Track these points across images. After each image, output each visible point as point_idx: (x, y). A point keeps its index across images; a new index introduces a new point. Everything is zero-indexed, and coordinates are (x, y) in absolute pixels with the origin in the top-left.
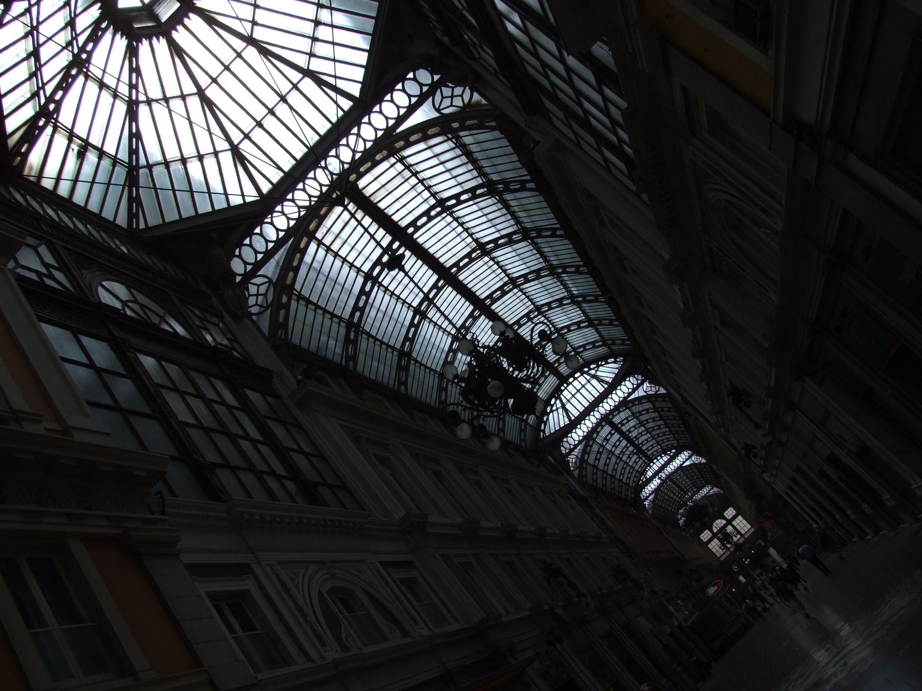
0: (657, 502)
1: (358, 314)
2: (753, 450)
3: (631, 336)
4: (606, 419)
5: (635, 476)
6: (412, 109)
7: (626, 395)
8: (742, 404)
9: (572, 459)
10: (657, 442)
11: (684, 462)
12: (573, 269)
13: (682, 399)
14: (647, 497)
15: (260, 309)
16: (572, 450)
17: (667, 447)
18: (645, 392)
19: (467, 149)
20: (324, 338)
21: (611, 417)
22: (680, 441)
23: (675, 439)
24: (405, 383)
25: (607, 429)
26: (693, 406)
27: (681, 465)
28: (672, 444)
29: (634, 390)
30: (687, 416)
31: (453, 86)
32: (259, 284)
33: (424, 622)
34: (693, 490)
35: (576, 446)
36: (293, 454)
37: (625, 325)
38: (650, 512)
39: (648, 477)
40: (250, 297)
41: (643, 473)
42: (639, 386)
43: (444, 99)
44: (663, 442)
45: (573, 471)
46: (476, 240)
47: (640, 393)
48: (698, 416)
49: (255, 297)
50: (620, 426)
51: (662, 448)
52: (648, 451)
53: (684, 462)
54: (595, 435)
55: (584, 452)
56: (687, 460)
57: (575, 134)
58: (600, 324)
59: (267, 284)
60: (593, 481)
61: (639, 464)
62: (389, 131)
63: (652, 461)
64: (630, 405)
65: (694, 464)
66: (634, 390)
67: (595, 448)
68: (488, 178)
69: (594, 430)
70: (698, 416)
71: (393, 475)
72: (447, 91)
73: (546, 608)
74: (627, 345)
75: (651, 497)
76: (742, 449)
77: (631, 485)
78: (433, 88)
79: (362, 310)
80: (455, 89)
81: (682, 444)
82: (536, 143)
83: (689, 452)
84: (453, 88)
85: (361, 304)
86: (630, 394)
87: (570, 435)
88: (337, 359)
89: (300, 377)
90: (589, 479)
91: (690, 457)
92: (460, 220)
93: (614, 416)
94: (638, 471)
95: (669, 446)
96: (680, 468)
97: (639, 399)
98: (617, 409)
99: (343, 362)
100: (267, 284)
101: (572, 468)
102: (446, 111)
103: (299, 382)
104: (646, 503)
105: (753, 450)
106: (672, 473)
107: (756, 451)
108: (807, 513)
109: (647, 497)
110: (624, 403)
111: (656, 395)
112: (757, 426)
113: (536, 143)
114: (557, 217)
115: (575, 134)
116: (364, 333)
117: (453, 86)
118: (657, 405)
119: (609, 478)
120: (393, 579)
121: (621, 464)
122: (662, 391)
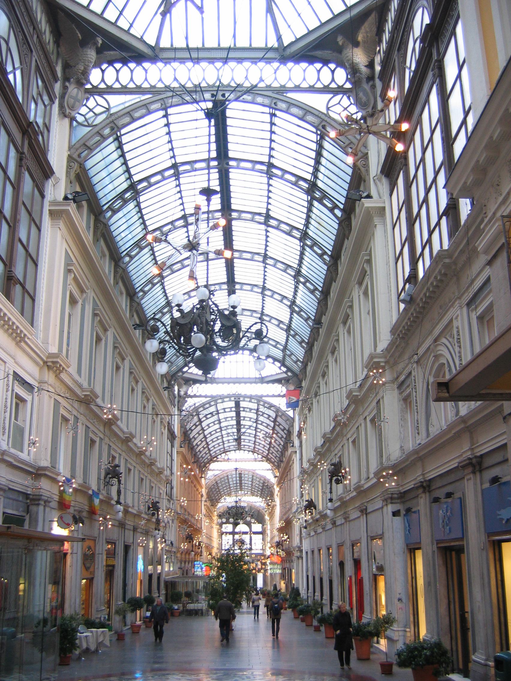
1: (145, 184)
2: (312, 508)
3: (305, 364)
5: (220, 449)
6: (312, 89)
8: (335, 478)
9: (190, 403)
10: (255, 441)
12: (312, 287)
13: (298, 432)
15: (84, 121)
16: (195, 396)
17: (258, 451)
19: (321, 151)
20: (104, 174)
22: (270, 454)
24: (132, 258)
25: (233, 404)
26: (301, 442)
28: (264, 452)
29: (274, 396)
31: (353, 103)
32: (99, 103)
33: (9, 437)
36: (20, 246)
37: (309, 351)
38: (207, 481)
40: (85, 107)
41: (225, 452)
42: (279, 396)
43: (338, 105)
44: (259, 445)
45: (183, 410)
46: (268, 210)
48: (298, 452)
49: (89, 110)
50: (241, 409)
51: (254, 448)
52: (244, 442)
54: (220, 401)
55: (203, 405)
57: (398, 218)
58: (294, 336)
59: (105, 109)
60: (190, 429)
61: (230, 444)
62: (283, 90)
63: (239, 448)
67: (213, 409)
68: (316, 181)
69: (222, 398)
70: (298, 452)
71: (70, 315)
72: (345, 102)
73: (90, 492)
74: (297, 365)
76: (306, 501)
77: (211, 452)
78: (340, 90)
79: (150, 185)
80: (352, 105)
82: (369, 196)
84: (351, 104)
85: (153, 180)
88: (103, 202)
89: (70, 196)
92: (271, 188)
93: (244, 401)
94: (224, 448)
95: (260, 451)
97: (271, 406)
98: (251, 397)
99: (105, 207)
100: (105, 109)
101: (184, 408)
102: (331, 114)
103: (66, 198)
104: (210, 474)
105: (312, 508)
107: (314, 510)
108: (308, 576)
110: (259, 399)
111: (284, 414)
112: (331, 500)
113: (369, 196)
114: (334, 247)
115: (398, 218)
116: (137, 201)
117: (353, 103)
118: (279, 419)
119: (202, 436)
120: (13, 390)
121: (219, 434)
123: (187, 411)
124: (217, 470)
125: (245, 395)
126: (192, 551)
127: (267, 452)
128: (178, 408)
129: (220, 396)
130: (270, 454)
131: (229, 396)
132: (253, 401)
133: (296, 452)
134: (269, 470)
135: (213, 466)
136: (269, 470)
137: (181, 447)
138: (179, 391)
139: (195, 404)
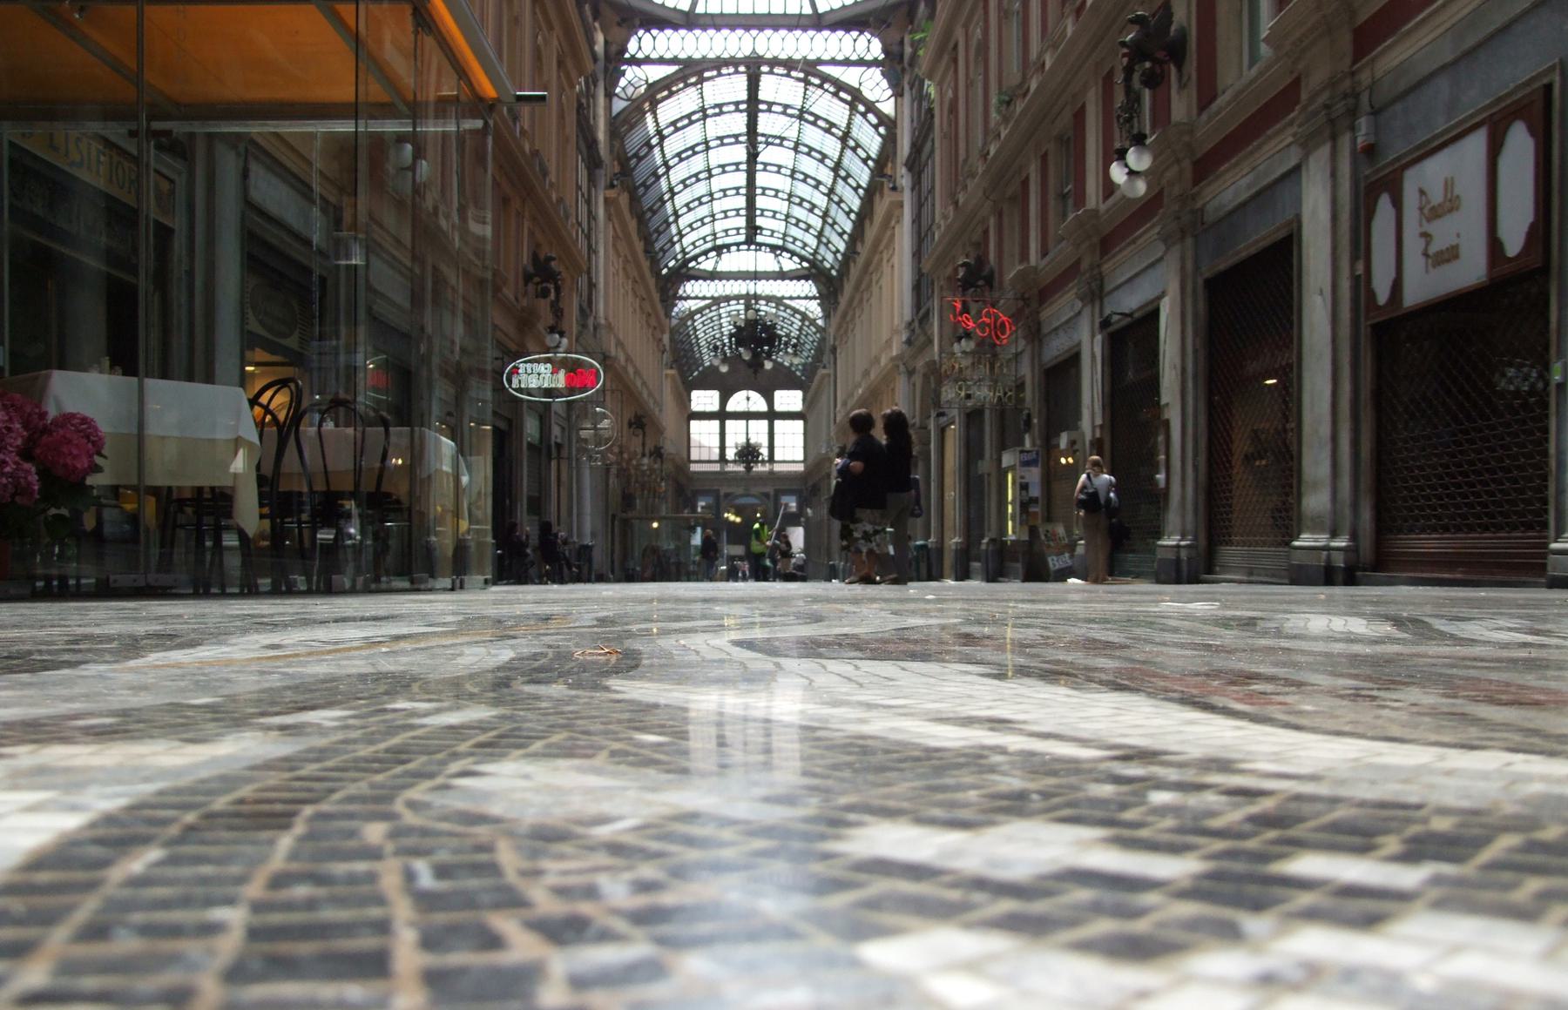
0: (696, 317)
4: (753, 67)
7: (826, 57)
10: (788, 216)
14: (688, 298)
16: (648, 60)
18: (860, 84)
21: (765, 69)
22: (822, 250)
23: (820, 235)
28: (805, 245)
29: (847, 63)
30: (891, 185)
34: (763, 351)
35: (662, 61)
39: (719, 269)
41: (719, 250)
42: (861, 62)
44: (793, 243)
47: (850, 76)
52: (762, 215)
53: (791, 298)
56: (799, 298)
60: (636, 155)
63: (750, 241)
64: (817, 81)
65: (804, 317)
66: (847, 63)
75: (693, 305)
77: (686, 241)
81: (820, 258)
83: (814, 291)
86: (833, 62)
87: (669, 32)
90: (633, 142)
93: (771, 72)
97: (840, 86)
98: (789, 65)
109: (688, 298)
110: (809, 70)
111: (871, 107)
122: (888, 108)
123: (628, 99)
124: (696, 298)
125: (775, 58)
126: (644, 455)
128: (606, 89)
129: (711, 60)
130: (822, 250)
131: (733, 62)
132: (794, 74)
133: (901, 205)
134: (814, 298)
135: (691, 288)
136: (814, 298)
137: (612, 186)
138: (606, 42)
139: (647, 81)
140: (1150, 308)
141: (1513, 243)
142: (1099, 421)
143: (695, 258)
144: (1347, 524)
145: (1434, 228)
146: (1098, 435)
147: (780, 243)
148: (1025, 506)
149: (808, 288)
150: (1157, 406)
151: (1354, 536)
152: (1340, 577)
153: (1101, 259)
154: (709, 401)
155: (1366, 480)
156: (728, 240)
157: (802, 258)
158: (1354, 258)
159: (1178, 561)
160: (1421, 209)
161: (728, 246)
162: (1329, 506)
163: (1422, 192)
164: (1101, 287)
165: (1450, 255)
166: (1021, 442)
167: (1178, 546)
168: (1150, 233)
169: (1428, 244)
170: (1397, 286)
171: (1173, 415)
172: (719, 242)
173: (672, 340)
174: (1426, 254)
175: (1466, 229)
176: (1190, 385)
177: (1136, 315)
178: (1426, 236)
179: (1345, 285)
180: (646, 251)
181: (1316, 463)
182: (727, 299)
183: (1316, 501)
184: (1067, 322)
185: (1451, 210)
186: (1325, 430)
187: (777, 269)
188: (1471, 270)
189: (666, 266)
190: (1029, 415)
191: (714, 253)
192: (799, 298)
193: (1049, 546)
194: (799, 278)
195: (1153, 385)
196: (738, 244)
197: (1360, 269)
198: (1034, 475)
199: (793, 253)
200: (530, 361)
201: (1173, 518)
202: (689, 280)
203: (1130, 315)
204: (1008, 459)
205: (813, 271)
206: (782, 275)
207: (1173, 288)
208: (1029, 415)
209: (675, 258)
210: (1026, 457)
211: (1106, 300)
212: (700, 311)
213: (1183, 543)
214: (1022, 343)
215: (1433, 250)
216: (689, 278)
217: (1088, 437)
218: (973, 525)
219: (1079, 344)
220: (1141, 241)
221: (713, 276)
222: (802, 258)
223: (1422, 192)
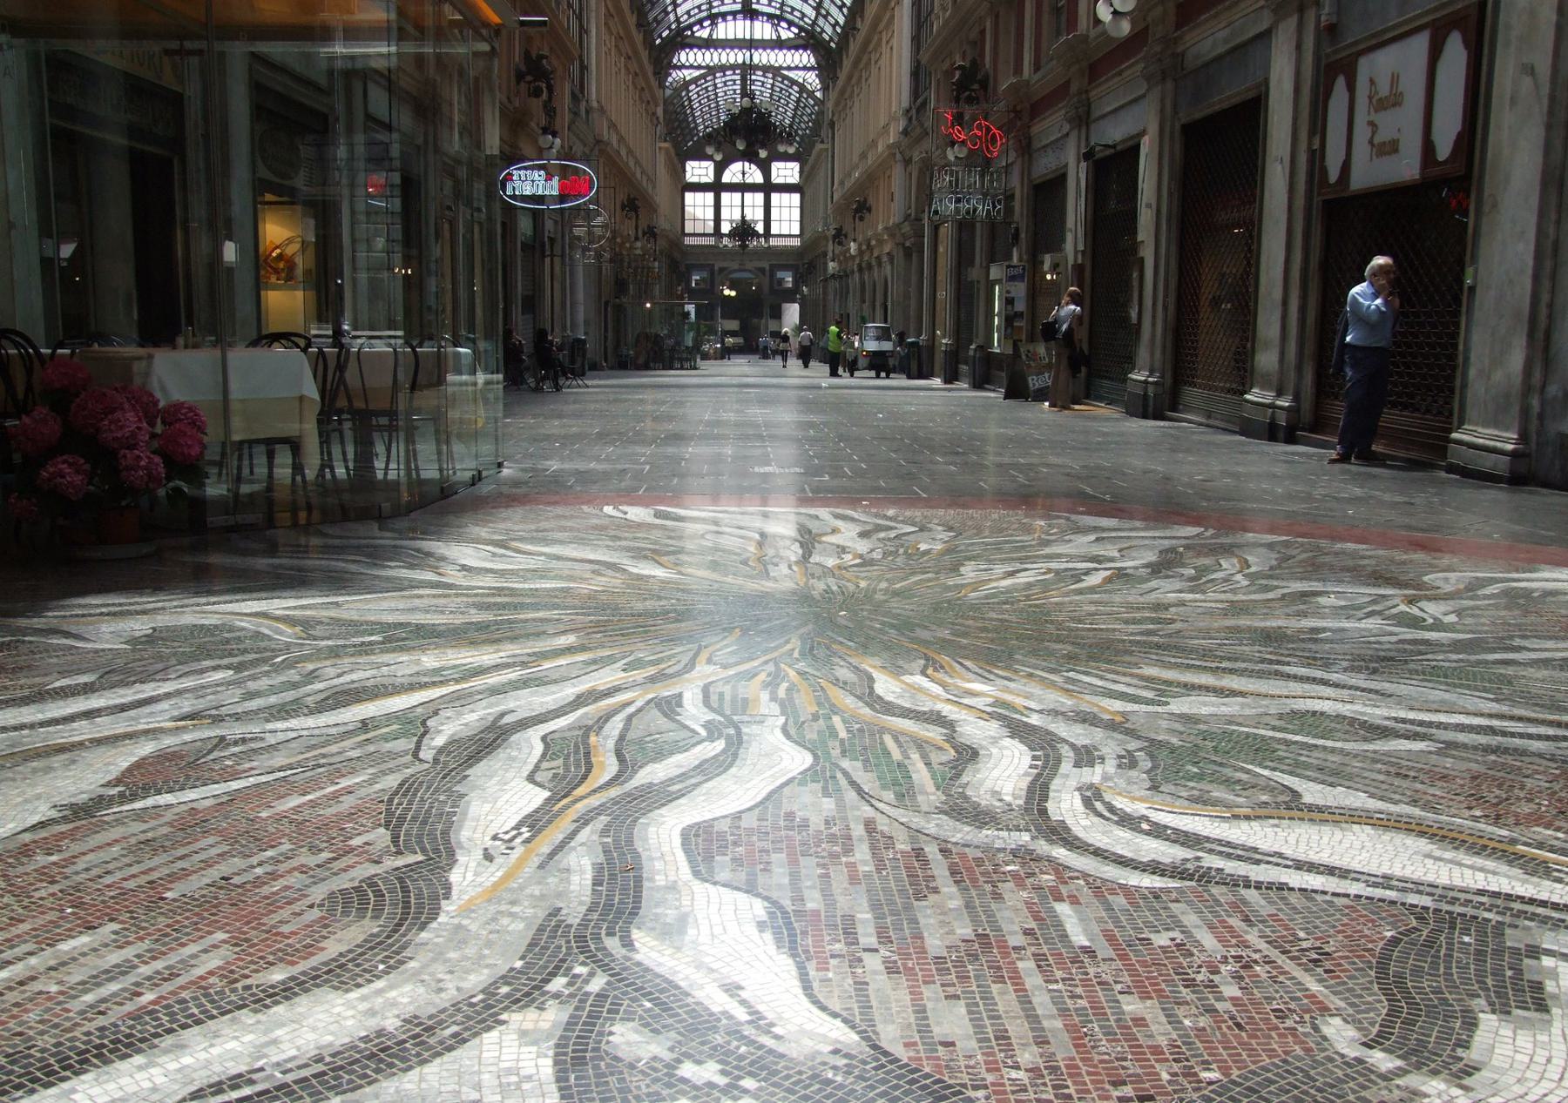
0: (691, 88)
11: (786, 69)
14: (683, 67)
22: (821, 21)
27: (781, 68)
28: (804, 15)
39: (714, 37)
41: (713, 18)
44: (791, 13)
53: (789, 68)
56: (797, 68)
65: (802, 88)
75: (689, 74)
77: (680, 11)
83: (812, 60)
91: (805, 68)
96: (775, 71)
106: (757, 67)
109: (683, 67)
124: (691, 67)
127: (813, 14)
130: (821, 21)
135: (684, 57)
136: (812, 68)
140: (1131, 143)
141: (1443, 151)
142: (1081, 247)
143: (690, 27)
144: (1291, 387)
145: (1378, 118)
146: (1080, 261)
147: (778, 12)
148: (1009, 320)
149: (805, 58)
150: (1135, 246)
151: (1297, 398)
152: (1281, 435)
153: (1089, 83)
154: (703, 172)
155: (1310, 348)
156: (724, 9)
157: (801, 29)
158: (1312, 134)
159: (1145, 395)
160: (1370, 98)
161: (724, 15)
162: (1277, 366)
163: (1372, 82)
164: (1088, 113)
165: (1390, 148)
166: (1009, 257)
167: (1146, 382)
168: (1134, 68)
169: (1374, 133)
170: (1346, 168)
171: (1147, 253)
172: (714, 11)
173: (665, 111)
174: (1371, 142)
175: (1404, 124)
176: (1164, 227)
177: (1119, 148)
178: (1372, 124)
179: (1303, 159)
180: (639, 25)
181: (1269, 325)
182: (723, 68)
183: (1267, 360)
184: (1057, 140)
185: (1394, 105)
186: (1277, 294)
187: (774, 37)
188: (1406, 168)
189: (660, 36)
190: (1017, 229)
191: (709, 22)
192: (797, 68)
193: (1029, 366)
194: (797, 48)
195: (1131, 217)
196: (734, 14)
197: (1316, 146)
198: (1020, 290)
199: (791, 24)
200: (526, 168)
201: (1143, 354)
202: (683, 48)
203: (1114, 147)
204: (995, 272)
205: (809, 39)
206: (779, 44)
207: (1153, 128)
208: (1017, 229)
209: (669, 28)
210: (1013, 272)
211: (1093, 127)
212: (695, 81)
213: (1150, 379)
214: (1012, 155)
215: (1377, 140)
216: (684, 46)
217: (1071, 262)
218: (963, 328)
219: (1066, 166)
220: (1125, 74)
221: (709, 44)
222: (801, 29)
223: (1372, 82)
